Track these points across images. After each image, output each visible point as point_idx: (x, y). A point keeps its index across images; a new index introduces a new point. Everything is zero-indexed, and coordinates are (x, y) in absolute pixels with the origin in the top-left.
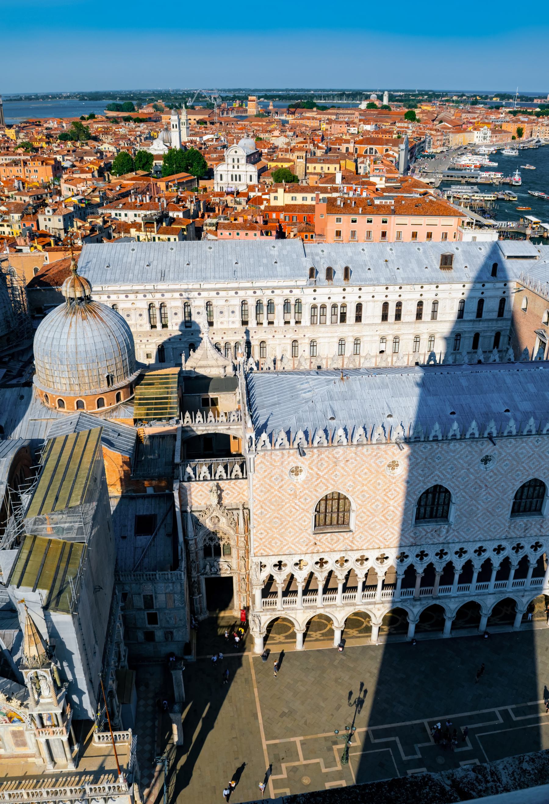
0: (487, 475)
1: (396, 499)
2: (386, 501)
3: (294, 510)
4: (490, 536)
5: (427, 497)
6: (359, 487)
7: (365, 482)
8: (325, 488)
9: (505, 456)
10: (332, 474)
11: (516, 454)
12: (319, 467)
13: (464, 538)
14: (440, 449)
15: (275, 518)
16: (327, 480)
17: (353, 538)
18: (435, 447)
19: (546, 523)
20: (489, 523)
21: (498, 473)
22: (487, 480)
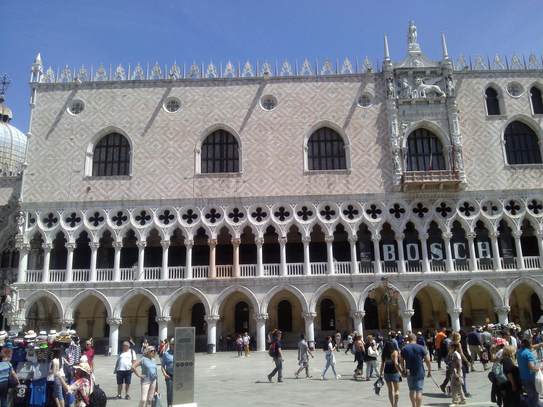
0: (271, 116)
1: (176, 139)
2: (165, 141)
3: (68, 147)
4: (288, 190)
5: (214, 147)
8: (101, 123)
9: (286, 96)
10: (109, 108)
12: (98, 101)
13: (258, 191)
15: (49, 156)
16: (104, 114)
17: (131, 184)
19: (352, 178)
20: (284, 174)
21: (282, 115)
22: (272, 122)
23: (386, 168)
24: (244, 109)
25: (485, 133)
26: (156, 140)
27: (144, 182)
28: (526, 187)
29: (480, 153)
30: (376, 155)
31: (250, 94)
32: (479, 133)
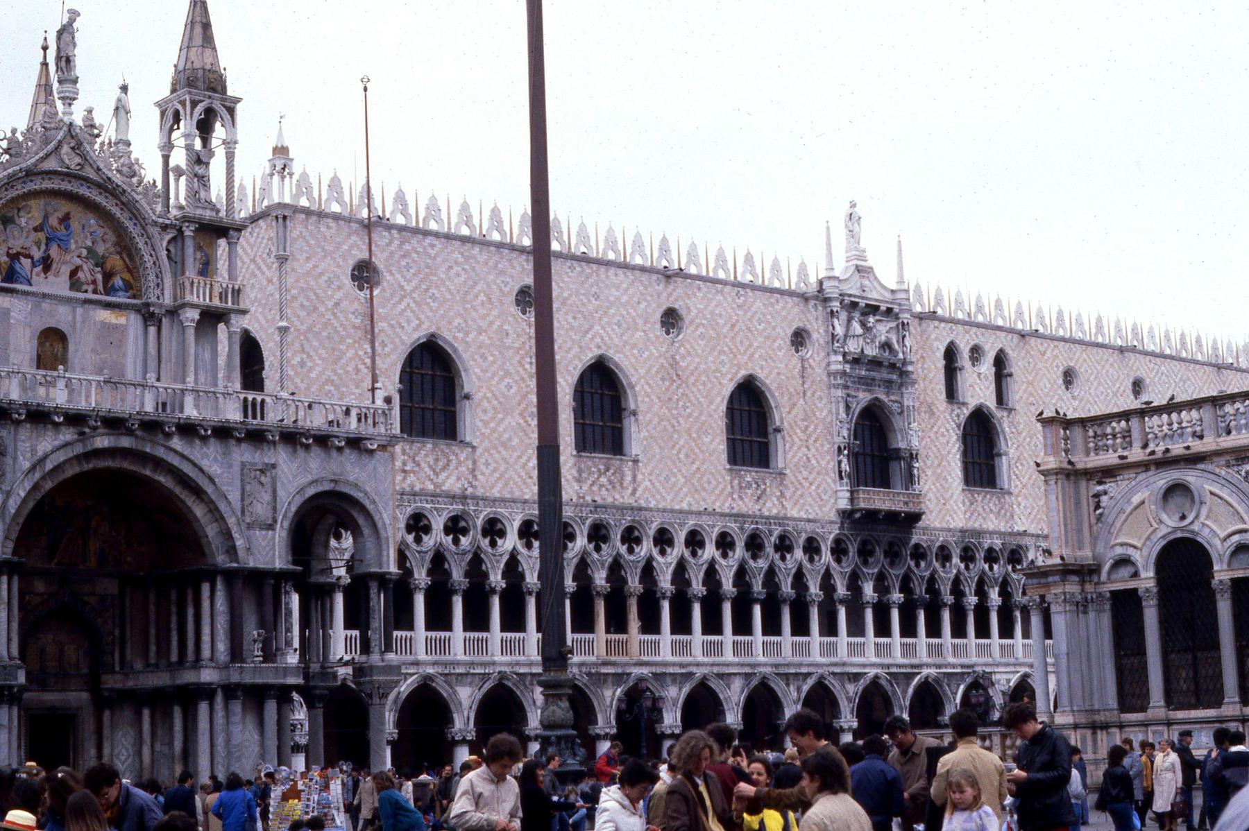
2: (523, 379)
6: (472, 335)
7: (484, 324)
8: (415, 323)
9: (697, 316)
11: (712, 313)
14: (594, 277)
17: (474, 462)
18: (588, 271)
19: (787, 488)
20: (698, 469)
23: (827, 474)
24: (637, 330)
25: (943, 430)
26: (507, 373)
27: (496, 462)
28: (985, 526)
29: (936, 463)
30: (817, 450)
31: (646, 300)
32: (935, 429)
